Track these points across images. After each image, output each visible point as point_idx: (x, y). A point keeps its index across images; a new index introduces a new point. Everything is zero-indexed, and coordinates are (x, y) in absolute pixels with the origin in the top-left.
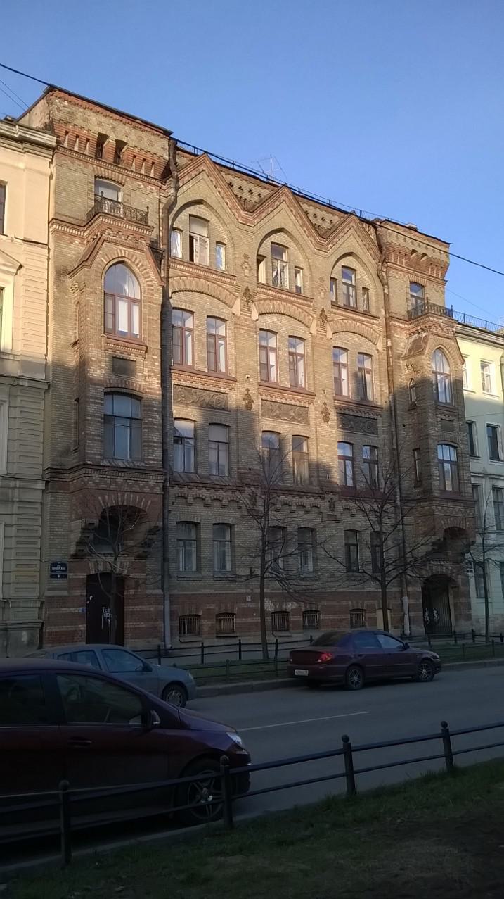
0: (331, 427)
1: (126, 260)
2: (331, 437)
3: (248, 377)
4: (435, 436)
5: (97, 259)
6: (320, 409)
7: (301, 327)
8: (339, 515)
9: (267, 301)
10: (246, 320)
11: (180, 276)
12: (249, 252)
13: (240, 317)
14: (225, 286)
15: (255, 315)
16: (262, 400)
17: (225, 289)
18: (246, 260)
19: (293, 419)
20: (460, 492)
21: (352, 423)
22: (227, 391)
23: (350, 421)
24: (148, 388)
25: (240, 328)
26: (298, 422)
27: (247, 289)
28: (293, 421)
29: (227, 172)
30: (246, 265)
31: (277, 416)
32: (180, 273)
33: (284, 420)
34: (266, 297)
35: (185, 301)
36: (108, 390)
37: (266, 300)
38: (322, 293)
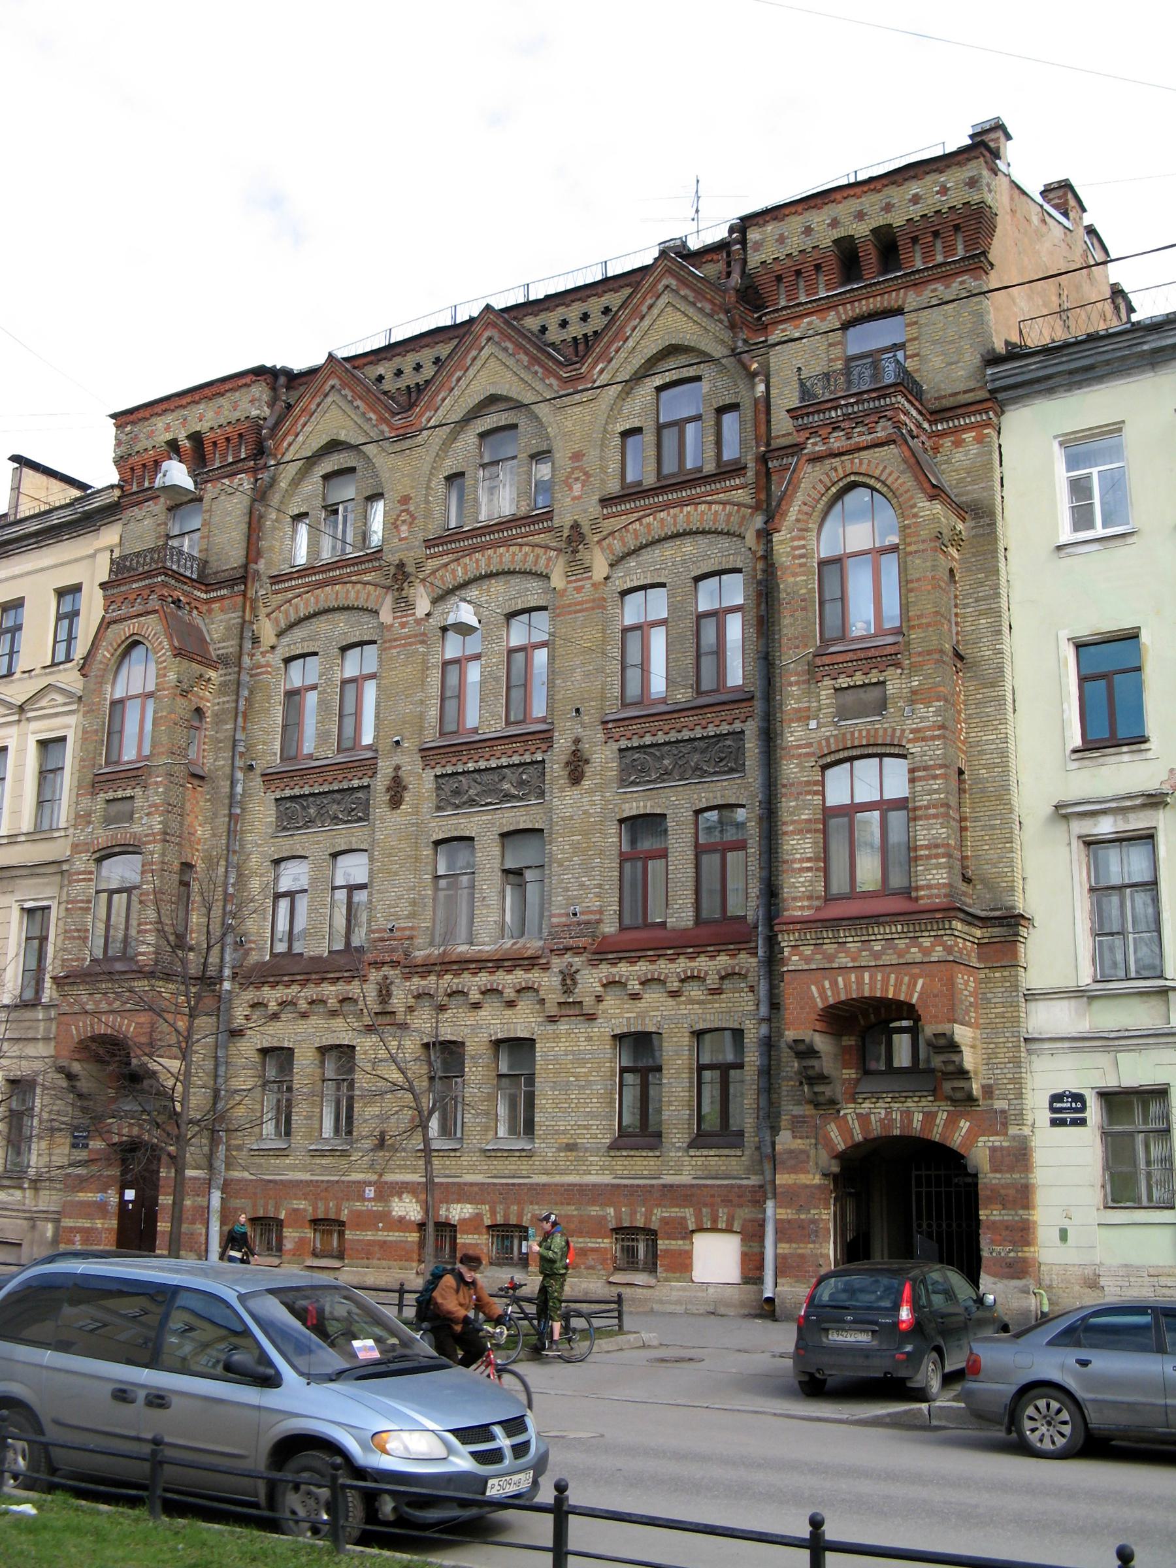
0: (590, 792)
1: (136, 638)
2: (591, 815)
3: (397, 742)
4: (809, 745)
5: (99, 657)
6: (564, 758)
7: (534, 584)
8: (588, 1001)
9: (452, 566)
10: (403, 625)
11: (289, 601)
12: (412, 487)
13: (392, 625)
14: (367, 578)
15: (423, 605)
16: (436, 776)
17: (366, 584)
18: (404, 507)
19: (508, 797)
20: (907, 893)
21: (666, 762)
22: (365, 782)
23: (662, 757)
24: (146, 836)
25: (390, 648)
26: (522, 799)
27: (401, 565)
28: (508, 801)
29: (389, 355)
30: (404, 516)
31: (472, 802)
32: (290, 595)
33: (487, 804)
34: (446, 559)
35: (303, 640)
36: (97, 855)
37: (446, 565)
38: (577, 487)
